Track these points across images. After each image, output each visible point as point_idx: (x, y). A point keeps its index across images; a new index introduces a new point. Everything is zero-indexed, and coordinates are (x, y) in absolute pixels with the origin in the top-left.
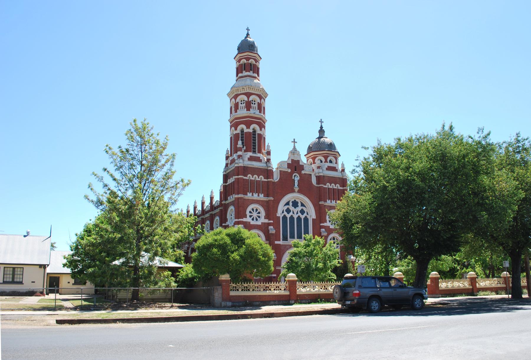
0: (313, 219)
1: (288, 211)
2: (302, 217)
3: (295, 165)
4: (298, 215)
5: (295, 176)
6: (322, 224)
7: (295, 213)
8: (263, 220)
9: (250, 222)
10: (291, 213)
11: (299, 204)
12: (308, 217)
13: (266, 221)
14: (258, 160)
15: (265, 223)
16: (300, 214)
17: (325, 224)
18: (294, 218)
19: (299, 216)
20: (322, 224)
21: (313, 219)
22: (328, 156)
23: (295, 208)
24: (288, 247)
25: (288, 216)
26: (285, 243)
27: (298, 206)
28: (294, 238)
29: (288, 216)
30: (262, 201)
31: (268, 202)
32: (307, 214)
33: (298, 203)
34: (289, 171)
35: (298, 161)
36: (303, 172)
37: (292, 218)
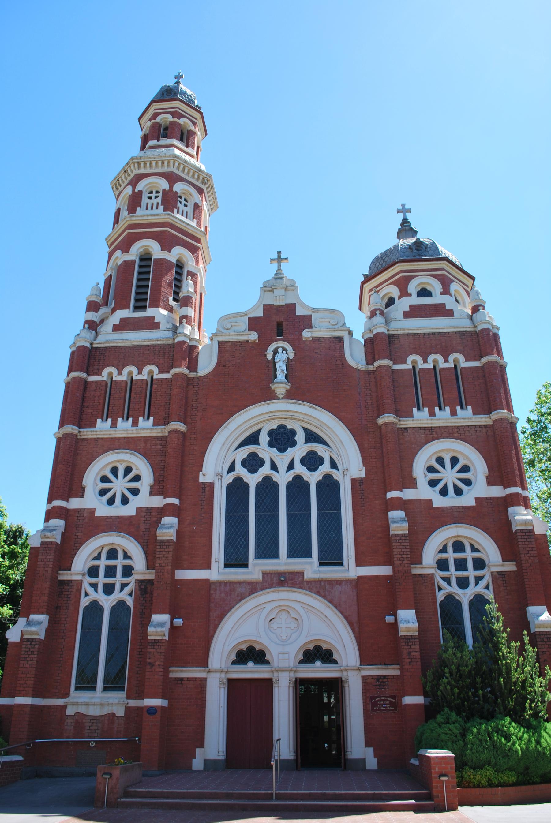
0: (354, 481)
1: (253, 463)
2: (313, 478)
3: (280, 321)
5: (275, 352)
6: (391, 494)
7: (282, 466)
8: (145, 500)
9: (92, 511)
11: (300, 437)
12: (337, 475)
13: (158, 502)
14: (151, 324)
15: (149, 510)
16: (300, 469)
17: (408, 494)
18: (275, 486)
19: (298, 479)
20: (391, 494)
21: (354, 481)
22: (408, 280)
23: (282, 450)
24: (240, 590)
25: (253, 480)
26: (237, 574)
27: (294, 444)
28: (276, 555)
29: (253, 480)
30: (146, 439)
31: (163, 440)
32: (334, 465)
33: (293, 433)
34: (253, 336)
35: (291, 307)
36: (307, 334)
37: (268, 487)
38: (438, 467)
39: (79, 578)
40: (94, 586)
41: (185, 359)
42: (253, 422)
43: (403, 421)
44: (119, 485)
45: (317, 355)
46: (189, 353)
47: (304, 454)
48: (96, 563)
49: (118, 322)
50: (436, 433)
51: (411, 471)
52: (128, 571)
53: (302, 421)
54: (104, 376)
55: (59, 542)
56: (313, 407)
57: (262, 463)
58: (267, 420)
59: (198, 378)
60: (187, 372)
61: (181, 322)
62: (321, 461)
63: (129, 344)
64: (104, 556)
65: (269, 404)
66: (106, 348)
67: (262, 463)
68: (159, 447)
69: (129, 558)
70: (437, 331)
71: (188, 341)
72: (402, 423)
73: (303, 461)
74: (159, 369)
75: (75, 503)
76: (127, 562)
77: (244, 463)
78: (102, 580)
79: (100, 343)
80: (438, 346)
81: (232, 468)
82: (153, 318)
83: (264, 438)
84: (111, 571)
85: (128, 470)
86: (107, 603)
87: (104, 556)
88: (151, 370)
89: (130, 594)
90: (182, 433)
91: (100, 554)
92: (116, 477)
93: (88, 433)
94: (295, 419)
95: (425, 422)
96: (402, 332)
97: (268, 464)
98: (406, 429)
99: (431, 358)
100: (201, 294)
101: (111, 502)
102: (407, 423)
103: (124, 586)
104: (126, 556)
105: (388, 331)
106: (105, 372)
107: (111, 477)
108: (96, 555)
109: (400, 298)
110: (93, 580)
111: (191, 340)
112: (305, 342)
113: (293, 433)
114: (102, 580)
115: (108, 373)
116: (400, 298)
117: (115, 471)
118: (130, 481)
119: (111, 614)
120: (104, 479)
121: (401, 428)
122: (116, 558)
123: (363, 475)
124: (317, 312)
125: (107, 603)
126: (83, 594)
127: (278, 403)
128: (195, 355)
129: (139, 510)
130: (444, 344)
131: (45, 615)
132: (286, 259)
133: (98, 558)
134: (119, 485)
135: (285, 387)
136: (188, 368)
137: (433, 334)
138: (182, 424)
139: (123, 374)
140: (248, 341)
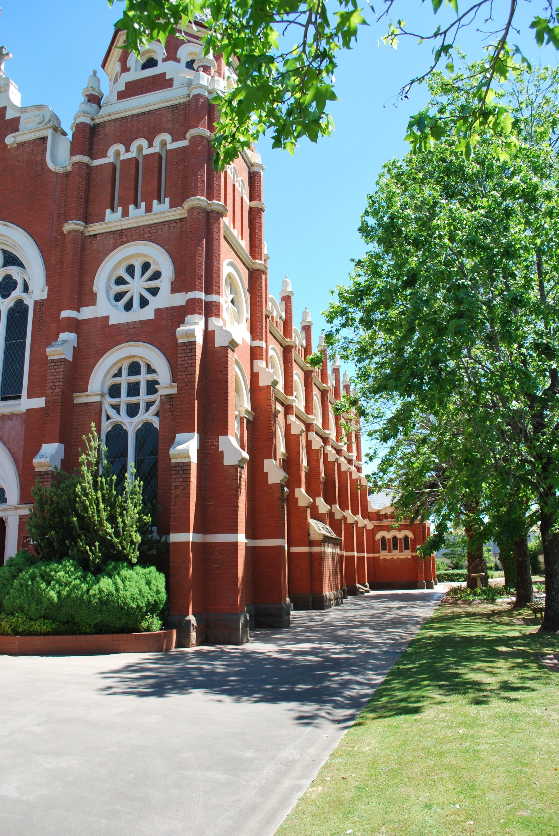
13: (180, 299)
39: (97, 399)
40: (116, 408)
44: (137, 286)
48: (117, 380)
49: (123, 88)
52: (152, 387)
54: (109, 159)
55: (70, 359)
64: (125, 372)
69: (153, 371)
71: (207, 94)
74: (172, 136)
75: (87, 313)
76: (151, 377)
78: (124, 399)
82: (164, 74)
84: (134, 390)
85: (146, 266)
86: (131, 426)
87: (125, 372)
88: (165, 142)
89: (157, 414)
91: (120, 370)
92: (133, 276)
93: (96, 228)
101: (128, 307)
103: (149, 405)
104: (150, 370)
106: (111, 152)
107: (127, 277)
108: (116, 372)
110: (115, 401)
111: (210, 92)
114: (124, 399)
115: (116, 153)
117: (130, 270)
118: (150, 279)
119: (136, 440)
120: (120, 281)
122: (138, 373)
125: (131, 426)
126: (104, 417)
129: (157, 311)
131: (58, 444)
133: (118, 374)
134: (137, 286)
139: (131, 150)
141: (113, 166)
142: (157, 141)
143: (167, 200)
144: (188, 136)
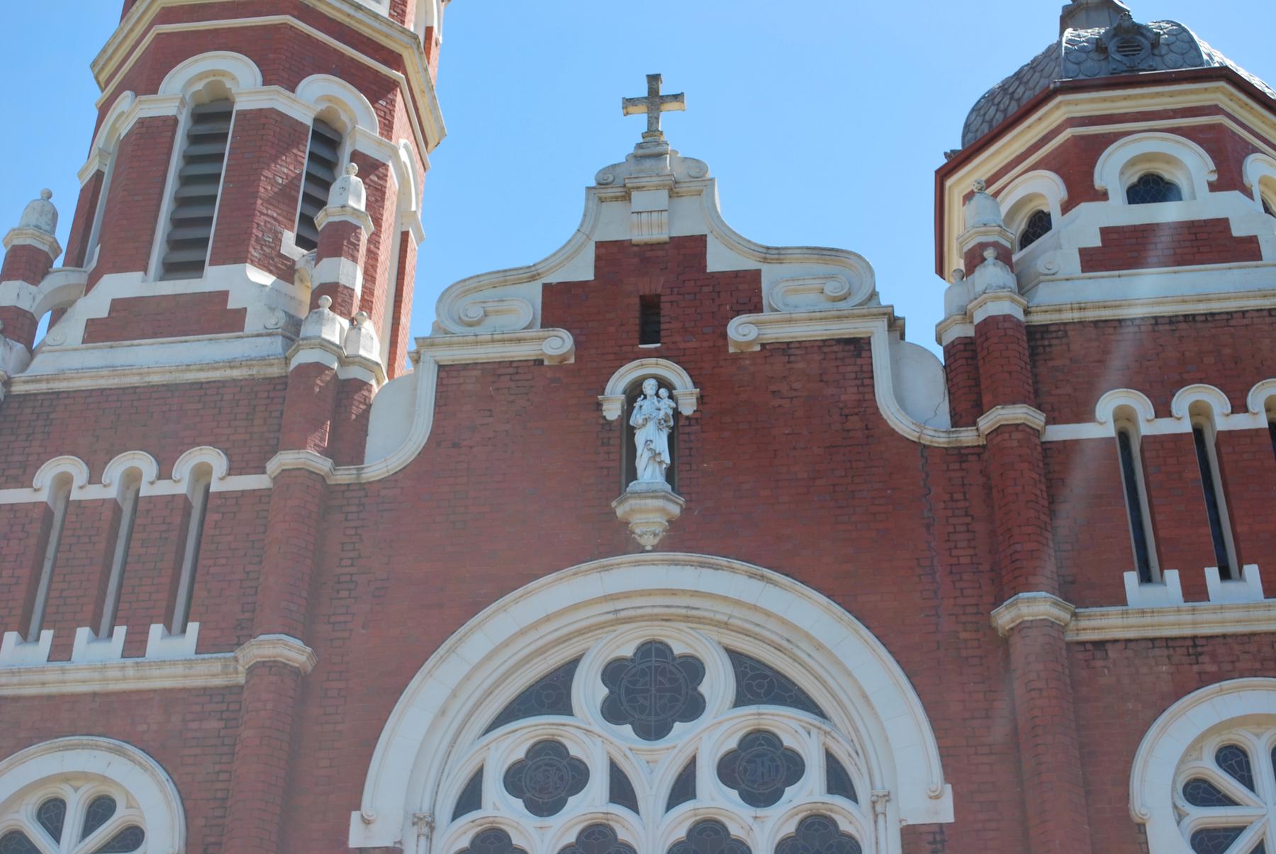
3: (649, 292)
4: (686, 813)
5: (634, 393)
7: (652, 786)
10: (590, 803)
11: (718, 683)
12: (850, 818)
14: (218, 316)
16: (716, 798)
22: (1095, 146)
23: (653, 730)
27: (694, 708)
30: (168, 698)
32: (839, 781)
33: (694, 668)
34: (559, 344)
35: (691, 249)
36: (742, 331)
38: (1227, 783)
41: (317, 425)
42: (549, 632)
43: (1089, 617)
45: (777, 402)
46: (338, 403)
47: (732, 744)
49: (104, 313)
50: (1214, 657)
51: (1126, 797)
53: (726, 625)
56: (762, 577)
57: (578, 776)
58: (601, 626)
59: (362, 486)
60: (323, 465)
61: (314, 305)
62: (793, 768)
63: (134, 380)
65: (605, 568)
66: (58, 394)
67: (578, 776)
68: (214, 724)
70: (1202, 308)
71: (336, 366)
72: (1084, 623)
73: (728, 770)
74: (230, 460)
77: (515, 780)
79: (36, 380)
80: (1209, 360)
81: (470, 798)
82: (224, 295)
83: (589, 691)
85: (100, 809)
88: (206, 465)
90: (296, 672)
94: (700, 620)
95: (1172, 618)
96: (1076, 316)
97: (599, 783)
98: (1100, 645)
99: (1183, 400)
100: (405, 236)
102: (1104, 623)
105: (1027, 312)
106: (46, 476)
109: (1066, 208)
111: (344, 361)
112: (736, 358)
113: (694, 668)
116: (1066, 208)
117: (51, 815)
121: (1083, 643)
123: (945, 813)
124: (780, 261)
127: (638, 563)
128: (356, 410)
130: (1227, 351)
132: (678, 97)
135: (662, 510)
136: (325, 453)
137: (1189, 318)
138: (298, 643)
139: (105, 478)
140: (539, 362)
141: (46, 512)
142: (184, 466)
143: (193, 627)
144: (274, 465)
